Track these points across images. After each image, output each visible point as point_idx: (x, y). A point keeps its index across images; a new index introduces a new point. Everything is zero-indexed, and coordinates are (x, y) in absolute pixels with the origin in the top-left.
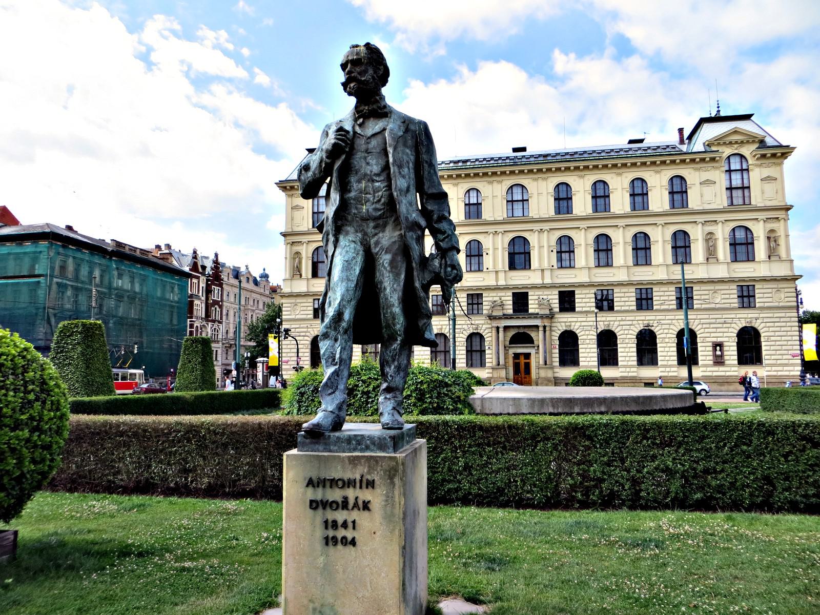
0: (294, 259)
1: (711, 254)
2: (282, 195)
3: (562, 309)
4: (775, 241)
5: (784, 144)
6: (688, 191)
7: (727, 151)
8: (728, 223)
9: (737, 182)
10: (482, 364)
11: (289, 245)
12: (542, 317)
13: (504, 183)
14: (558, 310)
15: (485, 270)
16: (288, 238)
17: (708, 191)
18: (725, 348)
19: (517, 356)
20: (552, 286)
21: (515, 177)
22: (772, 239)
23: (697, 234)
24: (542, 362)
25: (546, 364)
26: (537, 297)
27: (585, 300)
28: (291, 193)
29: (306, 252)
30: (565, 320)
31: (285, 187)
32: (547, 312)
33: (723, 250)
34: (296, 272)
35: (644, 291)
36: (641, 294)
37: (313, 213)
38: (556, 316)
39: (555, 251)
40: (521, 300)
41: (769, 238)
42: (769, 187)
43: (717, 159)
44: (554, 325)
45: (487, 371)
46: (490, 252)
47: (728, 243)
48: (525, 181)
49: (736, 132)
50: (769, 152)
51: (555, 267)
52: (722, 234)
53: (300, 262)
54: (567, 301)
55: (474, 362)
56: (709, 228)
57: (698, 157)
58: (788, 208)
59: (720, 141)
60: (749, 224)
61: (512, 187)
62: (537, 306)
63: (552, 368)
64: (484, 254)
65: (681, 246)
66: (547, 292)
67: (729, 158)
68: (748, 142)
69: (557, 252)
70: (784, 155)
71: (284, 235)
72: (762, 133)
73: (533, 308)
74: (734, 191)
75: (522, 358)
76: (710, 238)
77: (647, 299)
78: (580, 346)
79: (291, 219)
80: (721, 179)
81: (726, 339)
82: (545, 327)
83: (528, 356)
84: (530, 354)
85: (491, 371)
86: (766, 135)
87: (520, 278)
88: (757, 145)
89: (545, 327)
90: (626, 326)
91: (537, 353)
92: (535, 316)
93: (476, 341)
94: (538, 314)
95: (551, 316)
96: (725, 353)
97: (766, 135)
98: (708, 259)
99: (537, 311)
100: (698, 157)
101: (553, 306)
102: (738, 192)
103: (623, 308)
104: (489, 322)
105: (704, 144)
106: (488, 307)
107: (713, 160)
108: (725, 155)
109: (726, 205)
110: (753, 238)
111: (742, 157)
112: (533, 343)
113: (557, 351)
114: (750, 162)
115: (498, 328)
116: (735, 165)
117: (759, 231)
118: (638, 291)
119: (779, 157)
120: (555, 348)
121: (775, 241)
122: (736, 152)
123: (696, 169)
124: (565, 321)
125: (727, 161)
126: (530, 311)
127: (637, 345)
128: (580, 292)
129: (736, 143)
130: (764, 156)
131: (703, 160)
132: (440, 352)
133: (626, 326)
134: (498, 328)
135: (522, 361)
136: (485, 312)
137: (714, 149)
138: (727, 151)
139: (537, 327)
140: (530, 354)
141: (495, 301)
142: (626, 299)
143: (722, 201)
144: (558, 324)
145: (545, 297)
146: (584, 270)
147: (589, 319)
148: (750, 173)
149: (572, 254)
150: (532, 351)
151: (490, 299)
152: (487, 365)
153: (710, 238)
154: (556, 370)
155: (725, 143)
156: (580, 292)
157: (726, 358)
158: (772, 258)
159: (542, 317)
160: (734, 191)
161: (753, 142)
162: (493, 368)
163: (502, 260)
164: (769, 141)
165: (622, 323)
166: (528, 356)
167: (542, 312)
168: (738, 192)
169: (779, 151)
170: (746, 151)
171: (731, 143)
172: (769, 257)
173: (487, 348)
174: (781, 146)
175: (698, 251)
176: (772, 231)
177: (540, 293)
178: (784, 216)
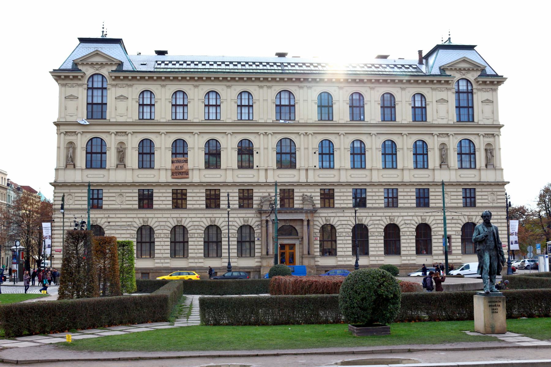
0: (68, 149)
1: (444, 161)
2: (54, 86)
3: (324, 207)
4: (491, 153)
5: (499, 75)
6: (427, 107)
7: (458, 76)
8: (457, 136)
9: (463, 103)
10: (252, 255)
11: (62, 135)
12: (307, 212)
13: (273, 88)
14: (319, 206)
15: (255, 167)
16: (61, 127)
17: (442, 108)
18: (453, 240)
19: (283, 246)
20: (316, 184)
21: (284, 84)
22: (489, 151)
23: (433, 144)
24: (306, 252)
25: (309, 254)
26: (301, 194)
27: (344, 198)
28: (64, 82)
29: (81, 142)
30: (326, 215)
31: (59, 77)
32: (310, 207)
33: (453, 159)
34: (70, 162)
35: (390, 191)
36: (388, 193)
37: (88, 104)
38: (318, 211)
39: (317, 153)
40: (287, 195)
41: (486, 150)
42: (487, 108)
43: (450, 82)
44: (315, 219)
45: (256, 260)
46: (262, 151)
47: (456, 153)
48: (292, 88)
49: (464, 60)
50: (488, 80)
51: (318, 167)
52: (453, 144)
53: (74, 152)
54: (328, 197)
55: (210, 252)
56: (444, 140)
57: (435, 79)
58: (500, 127)
59: (452, 67)
60: (472, 138)
61: (280, 92)
62: (301, 202)
63: (314, 257)
64: (255, 153)
65: (421, 152)
66: (311, 190)
67: (458, 81)
68: (473, 70)
69: (319, 154)
70: (499, 83)
71: (57, 124)
72: (483, 63)
73: (297, 203)
74: (461, 109)
75: (287, 248)
76: (443, 148)
77: (424, 198)
78: (370, 238)
79: (63, 108)
80: (452, 98)
81: (454, 233)
82: (308, 221)
83: (292, 246)
84: (295, 244)
85: (259, 260)
86: (486, 65)
87: (286, 176)
88: (479, 73)
89: (308, 221)
90: (376, 221)
91: (301, 243)
92: (300, 211)
93: (246, 231)
94: (302, 209)
95: (314, 211)
96: (453, 244)
97: (486, 65)
98: (440, 165)
99: (301, 206)
100: (435, 79)
101: (315, 202)
102: (465, 109)
103: (406, 205)
104: (259, 215)
105: (440, 68)
106: (258, 202)
107: (447, 82)
108: (456, 80)
109: (455, 121)
110: (475, 149)
111: (468, 81)
112: (297, 235)
113: (318, 242)
114: (474, 87)
115: (267, 221)
116: (463, 86)
117: (480, 144)
118: (386, 191)
119: (495, 85)
120: (316, 240)
121: (491, 153)
122: (464, 77)
123: (433, 89)
124: (323, 217)
125: (457, 84)
126: (296, 206)
127: (385, 237)
128: (338, 190)
129: (464, 69)
130: (484, 83)
131: (439, 82)
132: (213, 242)
133: (376, 221)
134: (267, 221)
135: (287, 251)
136: (255, 206)
137: (448, 73)
138: (458, 76)
139: (302, 220)
140: (295, 244)
141: (265, 197)
142: (377, 198)
143: (453, 117)
144: (320, 219)
145: (309, 194)
146: (343, 171)
147: (346, 214)
148: (475, 96)
149: (331, 156)
150: (297, 242)
151: (261, 194)
152: (256, 254)
153: (443, 148)
154: (317, 259)
155: (451, 69)
156: (338, 190)
157: (453, 248)
158: (488, 166)
159: (307, 212)
160: (461, 109)
161: (477, 70)
162: (261, 258)
163: (272, 159)
164: (489, 71)
165: (373, 218)
166: (292, 246)
167: (306, 207)
168: (465, 109)
169: (495, 80)
170: (472, 76)
171: (460, 69)
172: (486, 166)
173: (256, 239)
174: (497, 75)
175: (434, 159)
176: (489, 144)
177: (305, 190)
178: (497, 133)
